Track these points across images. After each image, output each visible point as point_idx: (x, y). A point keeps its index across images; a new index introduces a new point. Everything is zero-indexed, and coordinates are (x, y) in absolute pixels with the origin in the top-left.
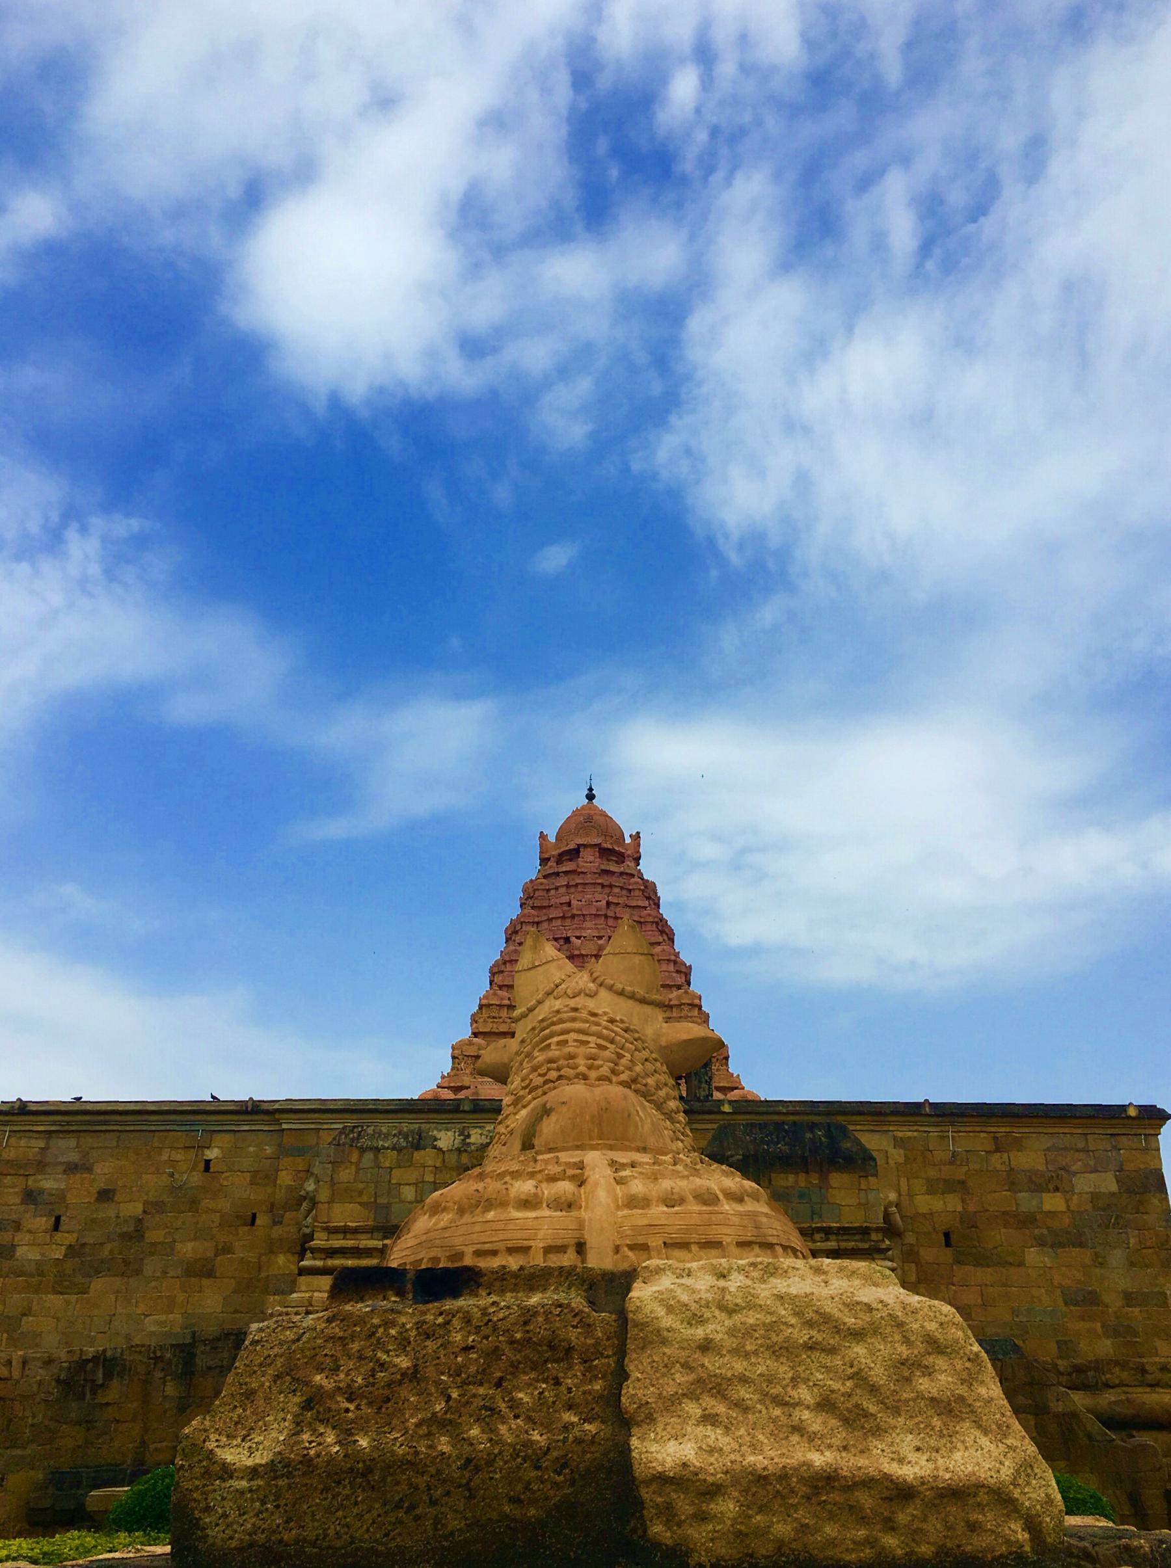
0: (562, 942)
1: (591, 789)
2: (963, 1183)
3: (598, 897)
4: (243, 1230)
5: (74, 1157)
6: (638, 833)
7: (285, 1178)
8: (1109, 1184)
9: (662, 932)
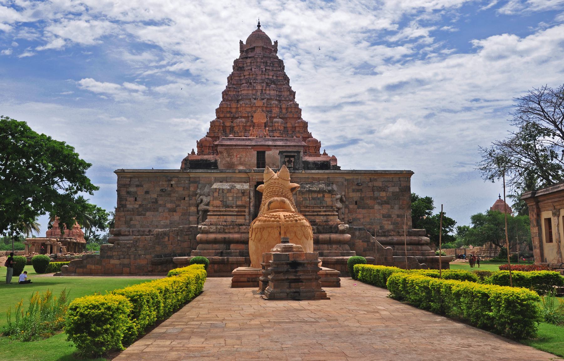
0: (249, 84)
1: (259, 23)
2: (361, 189)
3: (262, 67)
4: (182, 201)
5: (137, 183)
6: (277, 41)
7: (192, 189)
8: (397, 189)
9: (285, 80)
